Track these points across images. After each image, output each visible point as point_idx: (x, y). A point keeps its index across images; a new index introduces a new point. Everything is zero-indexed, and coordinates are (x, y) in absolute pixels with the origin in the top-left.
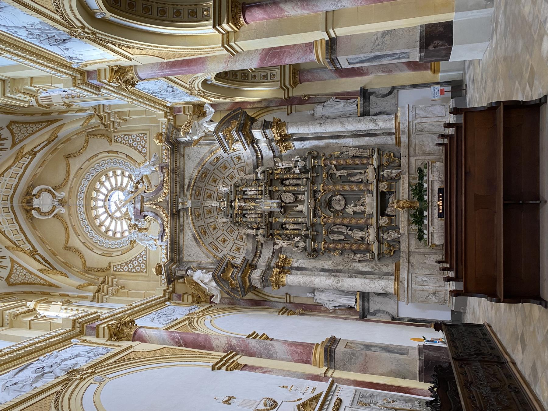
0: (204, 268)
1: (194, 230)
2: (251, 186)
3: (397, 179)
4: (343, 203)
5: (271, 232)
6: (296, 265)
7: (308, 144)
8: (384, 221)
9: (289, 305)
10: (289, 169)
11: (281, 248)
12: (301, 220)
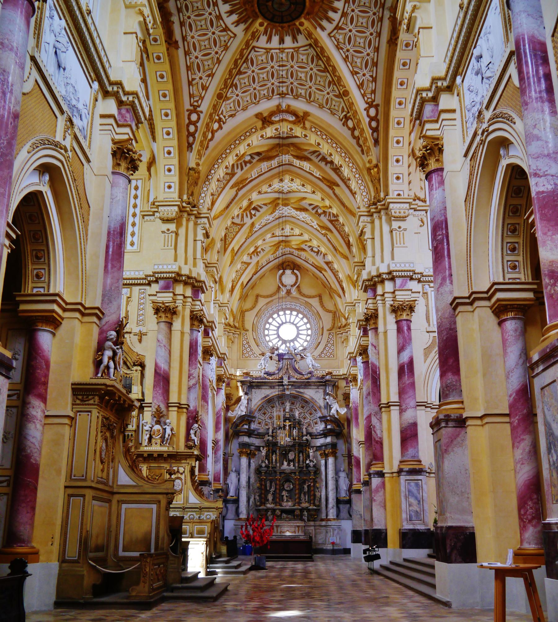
0: (248, 403)
1: (271, 395)
2: (299, 432)
3: (302, 520)
4: (288, 489)
5: (271, 446)
6: (252, 461)
7: (323, 468)
8: (278, 513)
9: (227, 456)
10: (308, 456)
11: (260, 451)
12: (278, 465)
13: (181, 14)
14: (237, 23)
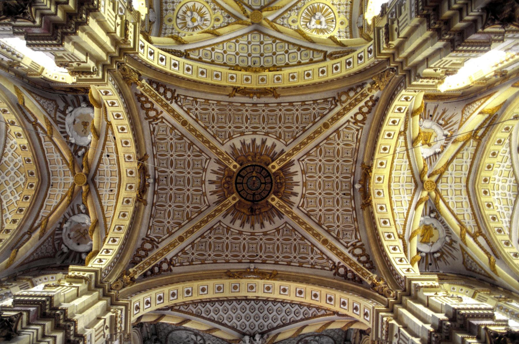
13: (251, 105)
14: (233, 148)
